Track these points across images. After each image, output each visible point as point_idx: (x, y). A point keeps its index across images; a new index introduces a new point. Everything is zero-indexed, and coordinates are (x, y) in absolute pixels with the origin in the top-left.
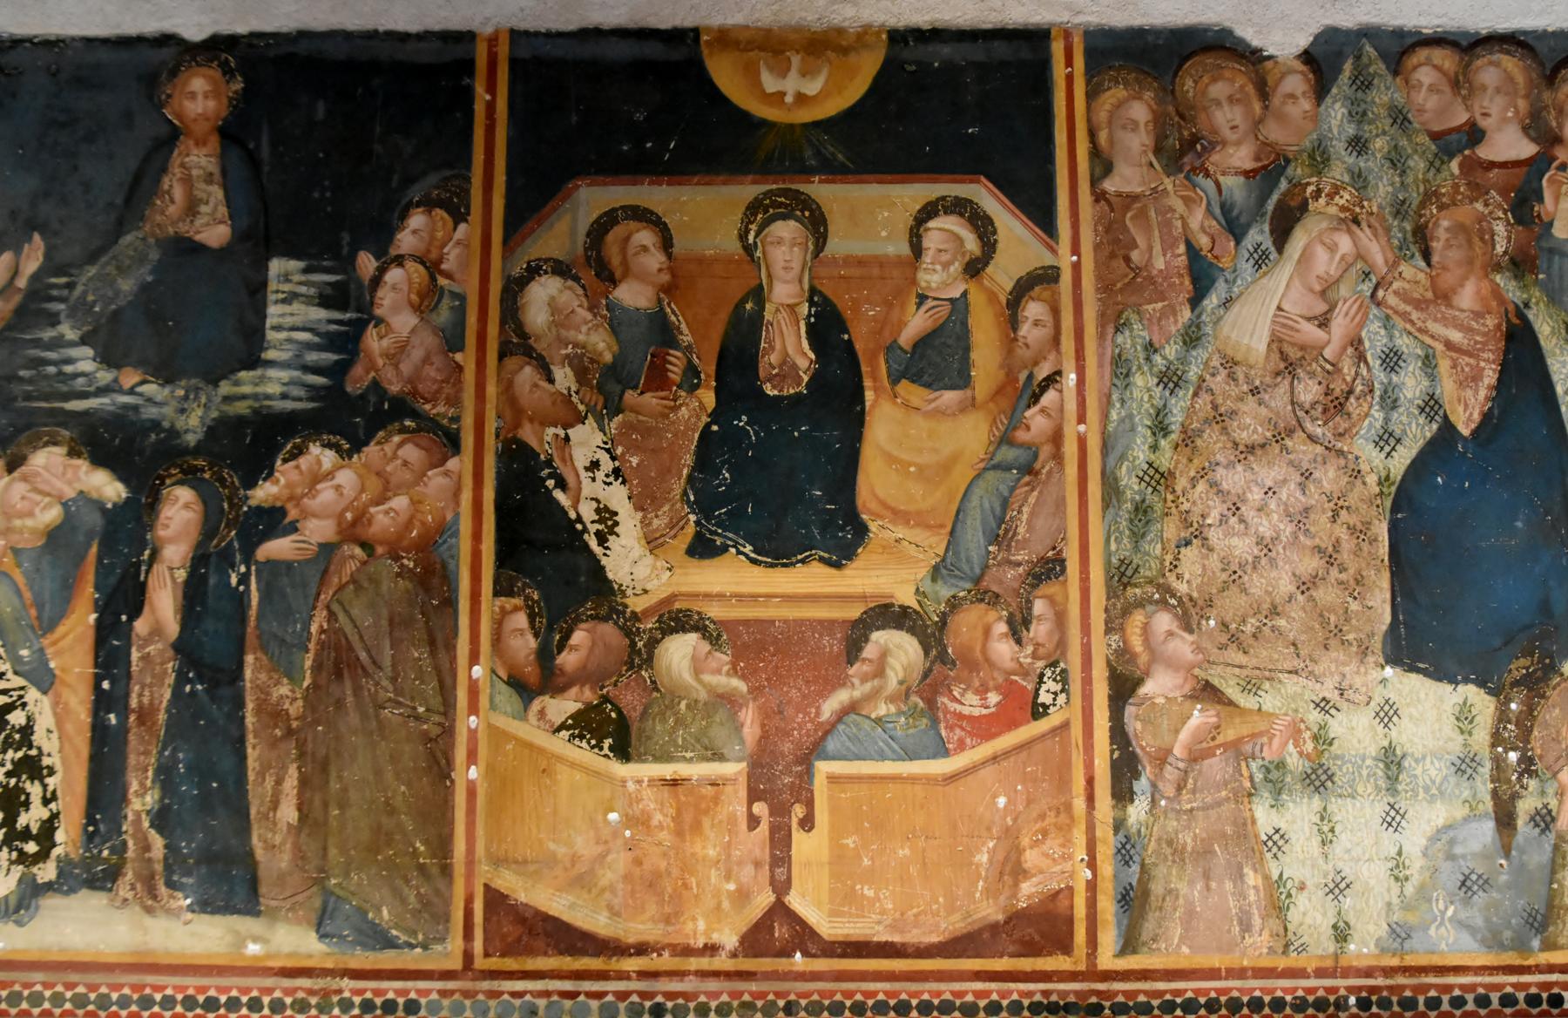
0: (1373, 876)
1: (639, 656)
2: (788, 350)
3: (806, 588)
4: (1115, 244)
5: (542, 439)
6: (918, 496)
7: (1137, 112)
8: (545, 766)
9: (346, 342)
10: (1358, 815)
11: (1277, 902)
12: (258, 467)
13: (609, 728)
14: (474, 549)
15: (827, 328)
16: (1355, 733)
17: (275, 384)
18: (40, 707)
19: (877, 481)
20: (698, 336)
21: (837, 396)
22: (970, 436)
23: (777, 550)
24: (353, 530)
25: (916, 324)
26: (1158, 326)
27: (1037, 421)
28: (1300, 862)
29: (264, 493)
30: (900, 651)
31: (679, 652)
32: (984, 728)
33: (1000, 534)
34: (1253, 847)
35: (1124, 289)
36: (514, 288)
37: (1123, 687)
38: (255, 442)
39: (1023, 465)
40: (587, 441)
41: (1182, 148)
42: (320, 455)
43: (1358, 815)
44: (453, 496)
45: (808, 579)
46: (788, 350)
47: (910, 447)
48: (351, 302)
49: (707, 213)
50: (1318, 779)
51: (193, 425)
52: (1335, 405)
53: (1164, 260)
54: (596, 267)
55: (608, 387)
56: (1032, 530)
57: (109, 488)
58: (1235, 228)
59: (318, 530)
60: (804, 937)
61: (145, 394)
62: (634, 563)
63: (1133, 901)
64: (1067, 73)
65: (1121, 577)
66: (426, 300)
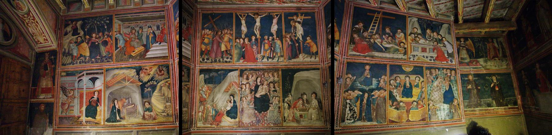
0: (443, 115)
1: (399, 104)
2: (408, 85)
3: (409, 100)
4: (427, 79)
5: (392, 90)
6: (416, 94)
7: (428, 72)
8: (393, 111)
9: (378, 84)
10: (442, 112)
11: (438, 117)
12: (372, 92)
13: (397, 109)
14: (387, 97)
15: (410, 84)
16: (442, 107)
17: (373, 86)
18: (356, 108)
19: (413, 93)
20: (403, 84)
21: (411, 88)
22: (419, 90)
23: (407, 97)
24: (379, 96)
25: (416, 84)
26: (430, 84)
27: (423, 90)
28: (439, 115)
29: (372, 94)
30: (415, 103)
31: (401, 104)
32: (420, 108)
33: (421, 96)
34: (436, 114)
35: (428, 82)
36: (390, 81)
37: (429, 105)
38: (372, 90)
39: (422, 92)
40: (395, 90)
41: (431, 73)
42: (377, 91)
43: (442, 112)
44: (386, 94)
45: (409, 99)
46: (408, 85)
47: (416, 91)
48: (379, 81)
49: (402, 77)
50: (440, 110)
51: (367, 89)
52: (440, 89)
53: (430, 80)
54: (395, 80)
55: (396, 87)
56: (423, 96)
57: (361, 93)
58: (434, 78)
59: (376, 96)
60: (410, 121)
61: (364, 87)
62: (399, 98)
63: (430, 118)
64: (424, 69)
65: (428, 99)
66: (384, 81)
